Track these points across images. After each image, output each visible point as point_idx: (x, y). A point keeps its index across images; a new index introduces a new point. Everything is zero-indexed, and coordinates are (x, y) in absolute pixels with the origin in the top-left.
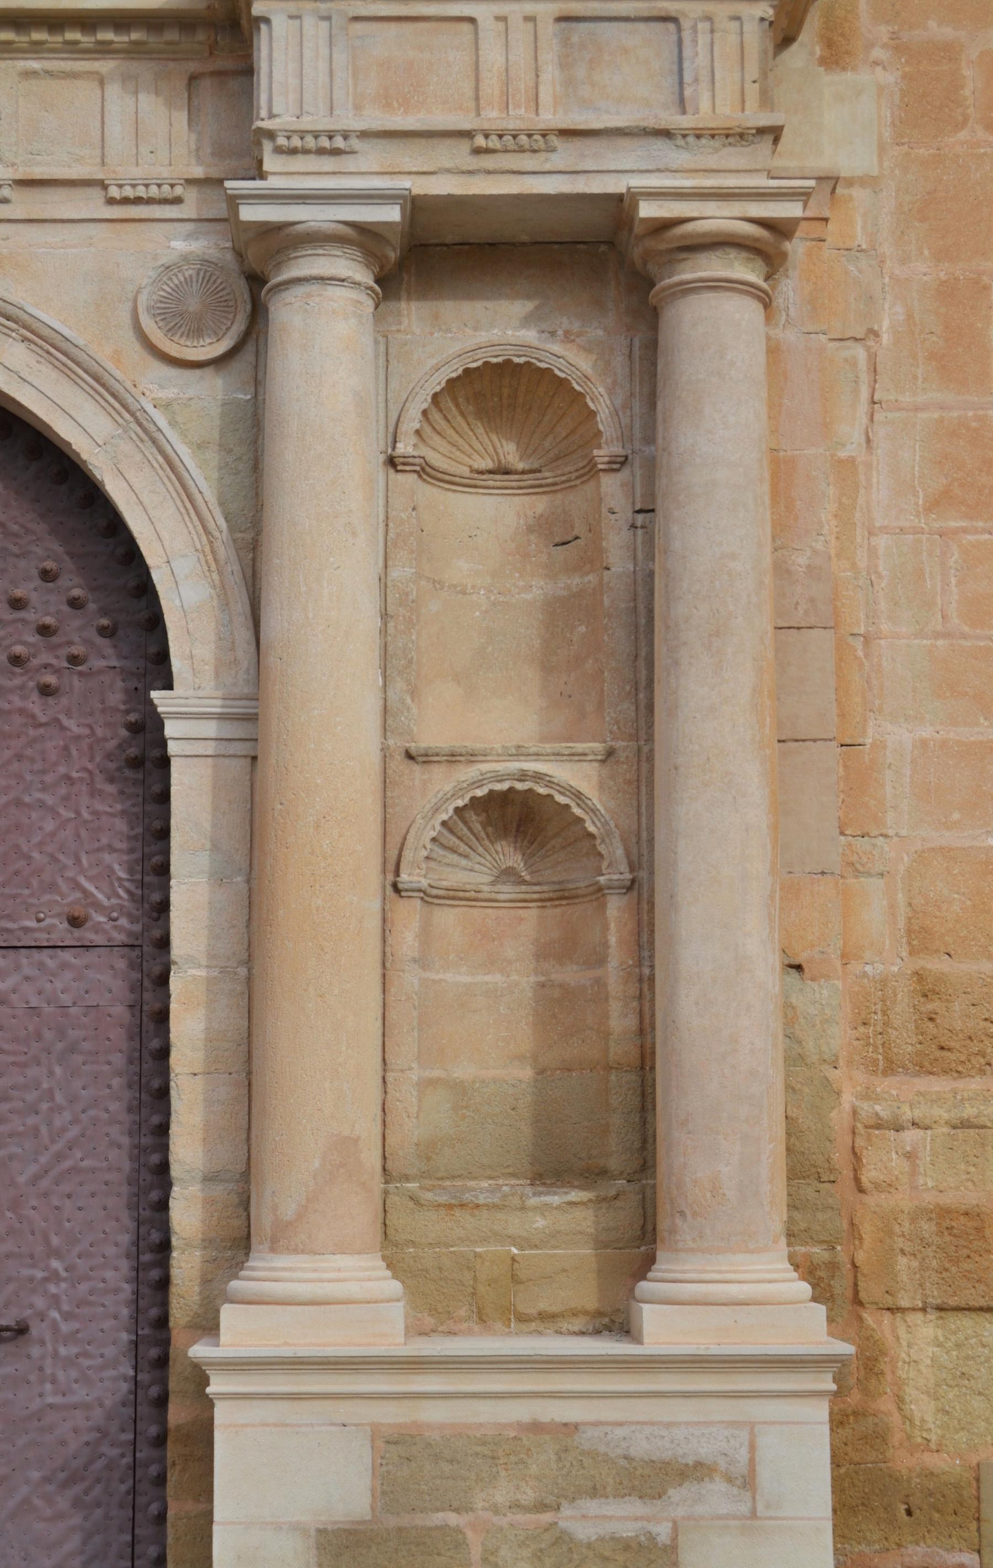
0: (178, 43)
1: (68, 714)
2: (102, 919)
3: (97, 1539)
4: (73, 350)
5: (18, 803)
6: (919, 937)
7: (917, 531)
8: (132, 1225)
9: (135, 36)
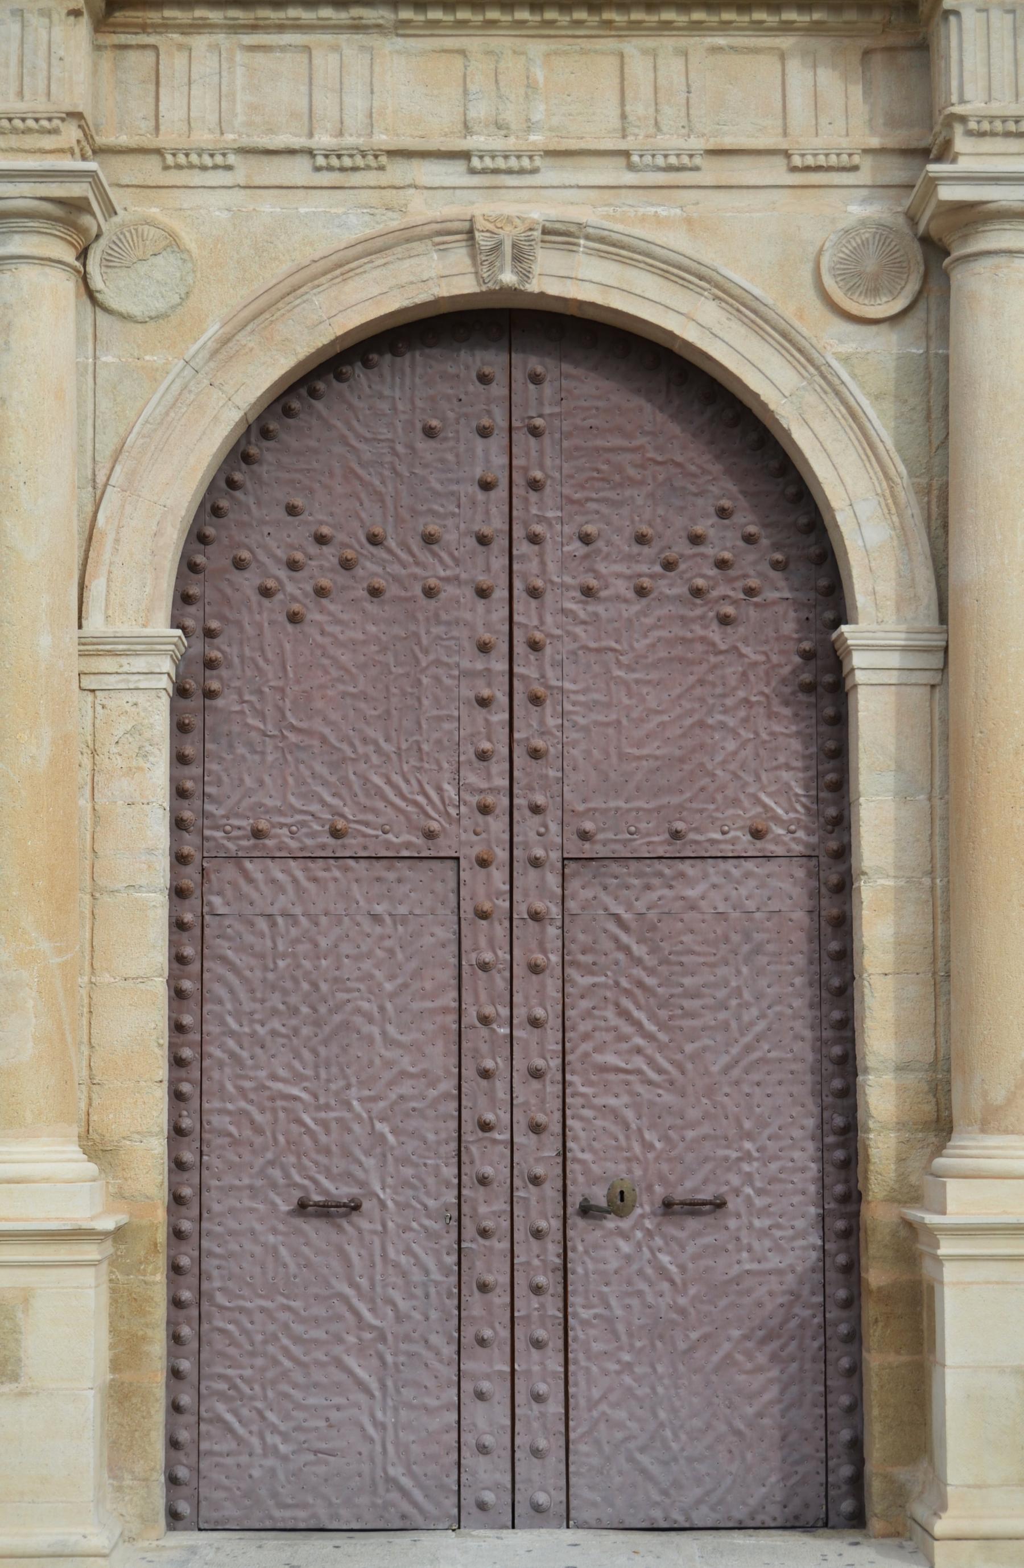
0: (855, 22)
1: (745, 641)
2: (781, 831)
3: (794, 1389)
4: (762, 308)
5: (701, 724)
8: (816, 1111)
9: (817, 16)
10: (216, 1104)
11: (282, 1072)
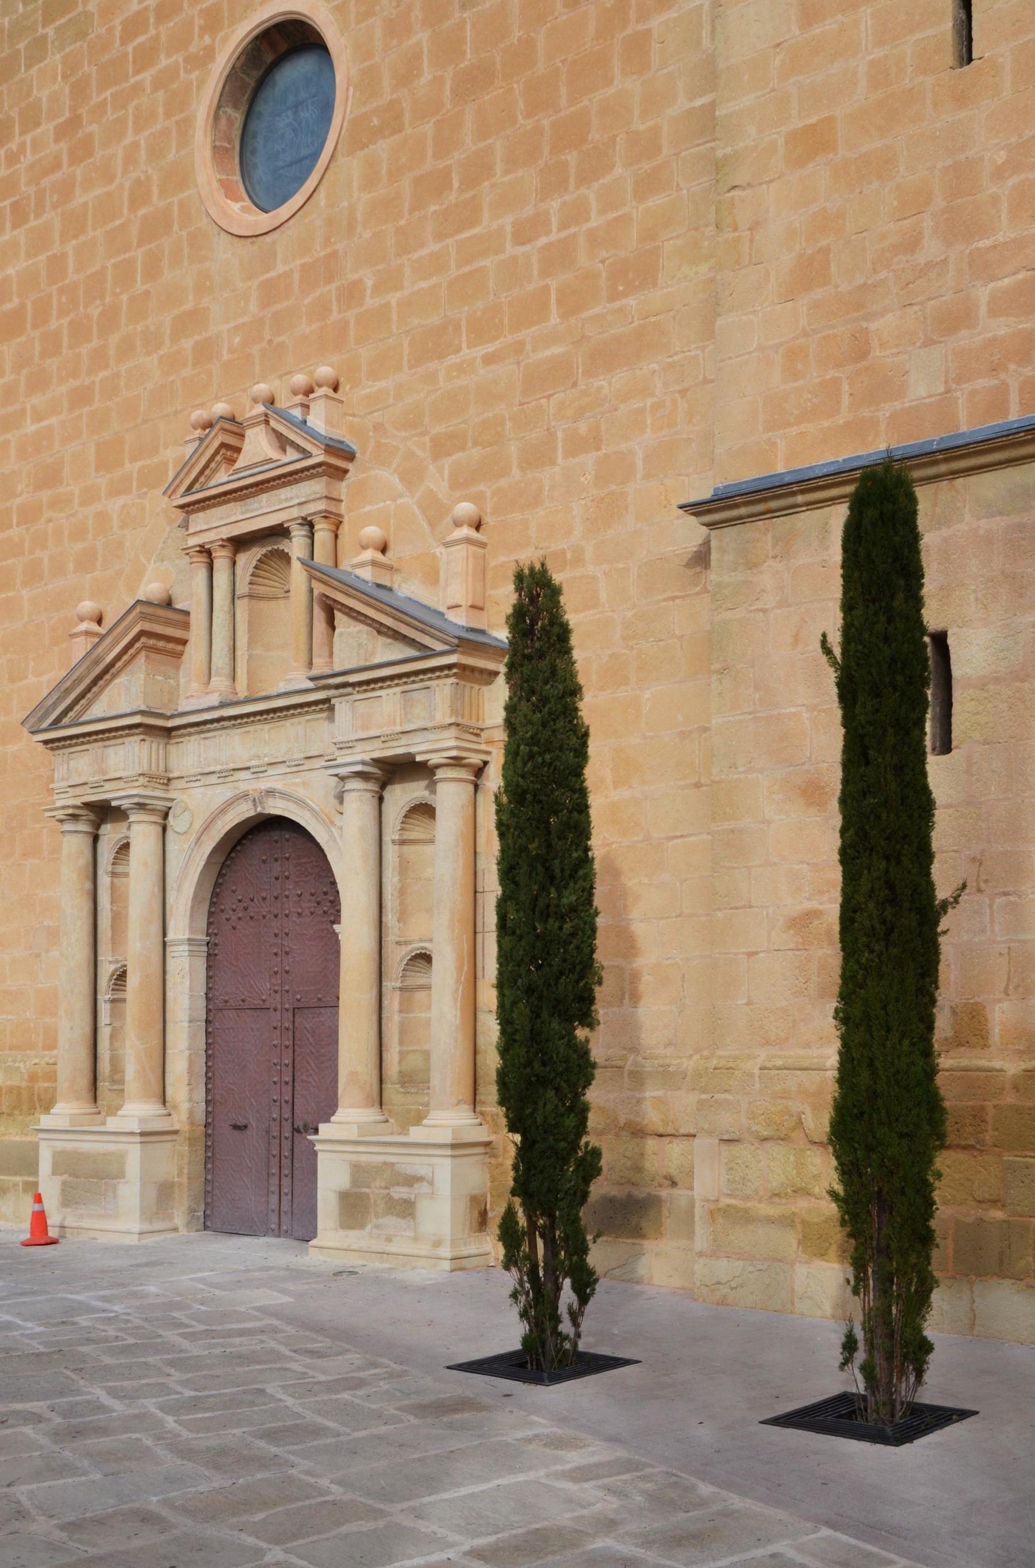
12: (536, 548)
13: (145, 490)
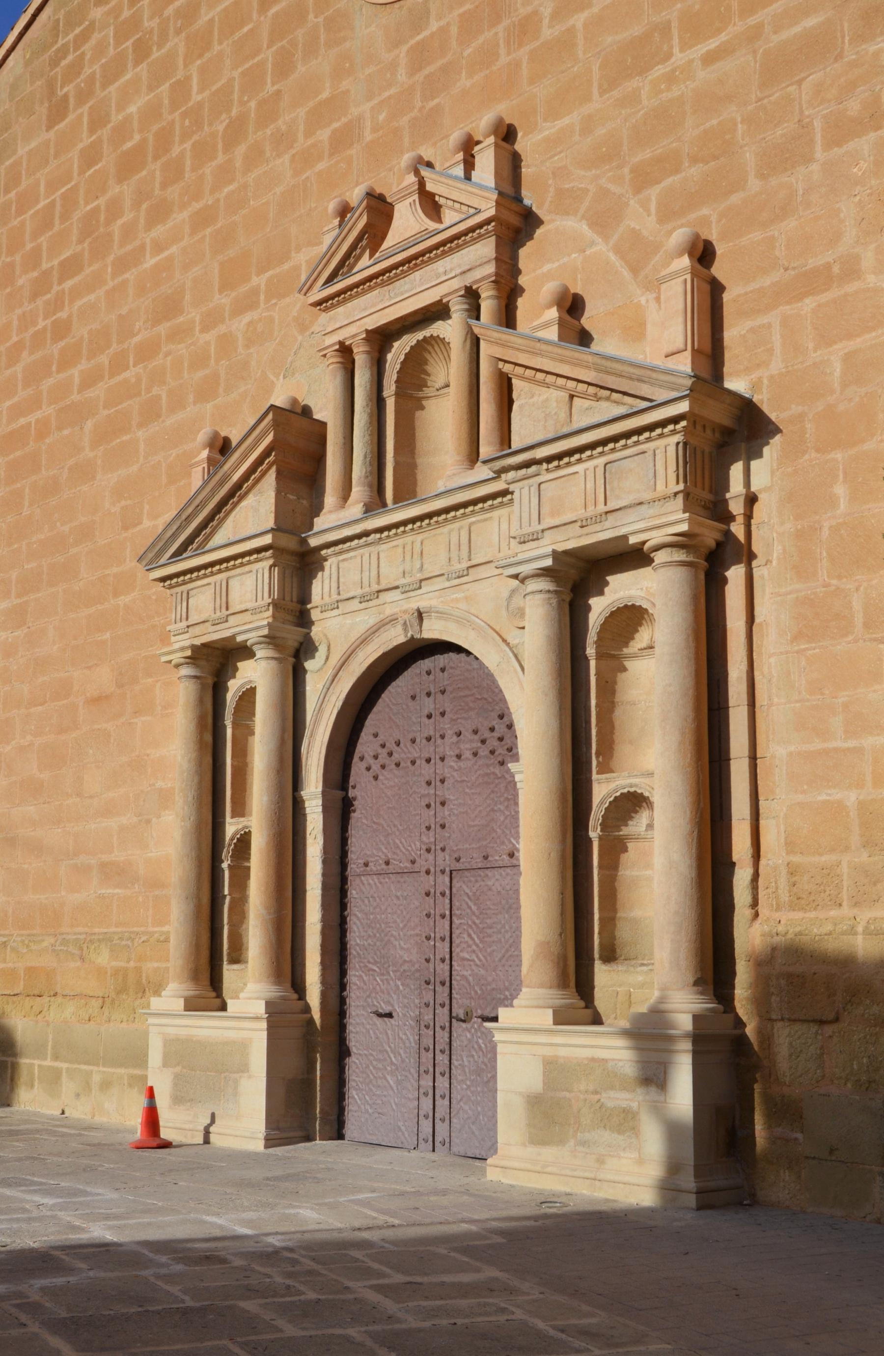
6: (790, 846)
7: (787, 653)
10: (353, 973)
11: (371, 960)
12: (786, 269)
13: (274, 301)
